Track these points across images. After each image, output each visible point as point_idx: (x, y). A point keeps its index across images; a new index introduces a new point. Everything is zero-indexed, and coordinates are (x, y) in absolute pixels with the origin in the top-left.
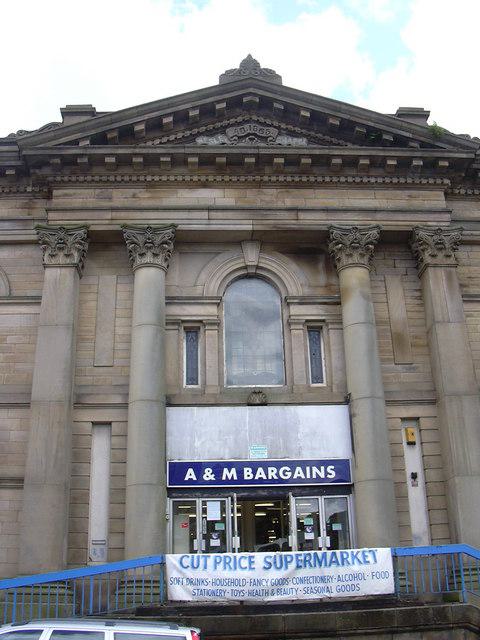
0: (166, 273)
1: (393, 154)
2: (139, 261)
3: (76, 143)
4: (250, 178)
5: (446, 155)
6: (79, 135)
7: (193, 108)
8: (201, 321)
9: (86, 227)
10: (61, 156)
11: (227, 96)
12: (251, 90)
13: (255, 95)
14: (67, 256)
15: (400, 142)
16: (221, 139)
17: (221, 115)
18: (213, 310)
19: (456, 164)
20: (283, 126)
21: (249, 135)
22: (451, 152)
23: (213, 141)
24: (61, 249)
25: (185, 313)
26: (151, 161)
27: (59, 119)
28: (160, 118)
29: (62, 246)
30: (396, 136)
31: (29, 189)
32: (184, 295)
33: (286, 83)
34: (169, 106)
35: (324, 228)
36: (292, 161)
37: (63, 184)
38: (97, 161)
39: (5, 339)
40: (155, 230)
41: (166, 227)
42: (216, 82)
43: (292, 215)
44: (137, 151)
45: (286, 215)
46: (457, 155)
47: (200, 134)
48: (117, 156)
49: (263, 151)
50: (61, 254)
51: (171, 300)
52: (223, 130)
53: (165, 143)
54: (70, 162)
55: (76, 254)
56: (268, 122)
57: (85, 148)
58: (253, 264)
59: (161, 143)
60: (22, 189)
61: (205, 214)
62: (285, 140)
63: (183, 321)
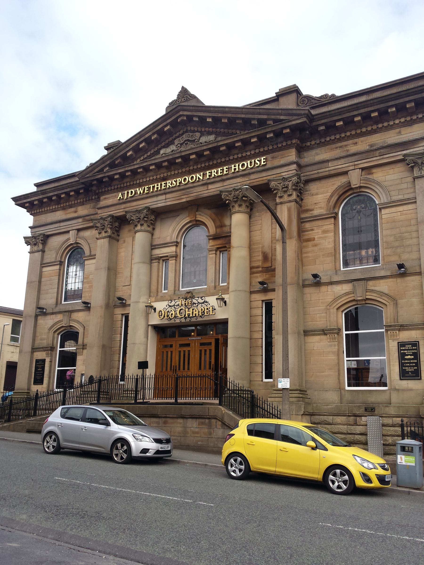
0: (250, 217)
1: (253, 134)
2: (278, 200)
3: (102, 170)
4: (184, 170)
5: (287, 124)
6: (103, 166)
7: (153, 134)
8: (167, 256)
9: (146, 207)
10: (97, 180)
11: (168, 121)
12: (181, 113)
13: (183, 115)
14: (106, 232)
15: (262, 123)
16: (173, 147)
17: (170, 133)
18: (173, 249)
19: (294, 129)
20: (203, 130)
21: (185, 141)
22: (291, 121)
23: (168, 150)
24: (103, 229)
25: (162, 252)
26: (134, 172)
27: (105, 152)
28: (138, 145)
29: (235, 200)
30: (259, 120)
31: (93, 198)
32: (162, 242)
33: (123, 141)
34: (141, 137)
35: (266, 181)
36: (215, 151)
37: (104, 193)
38: (111, 178)
39: (89, 277)
40: (139, 212)
41: (143, 209)
42: (164, 113)
43: (205, 188)
44: (127, 169)
45: (202, 188)
46: (294, 123)
47: (161, 149)
48: (119, 174)
49: (183, 154)
50: (103, 232)
51: (153, 247)
52: (172, 143)
53: (142, 160)
54: (100, 181)
55: (109, 231)
56: (196, 129)
57: (107, 172)
58: (357, 186)
59: (140, 161)
60: (90, 198)
61: (163, 197)
62: (203, 139)
63: (161, 257)
